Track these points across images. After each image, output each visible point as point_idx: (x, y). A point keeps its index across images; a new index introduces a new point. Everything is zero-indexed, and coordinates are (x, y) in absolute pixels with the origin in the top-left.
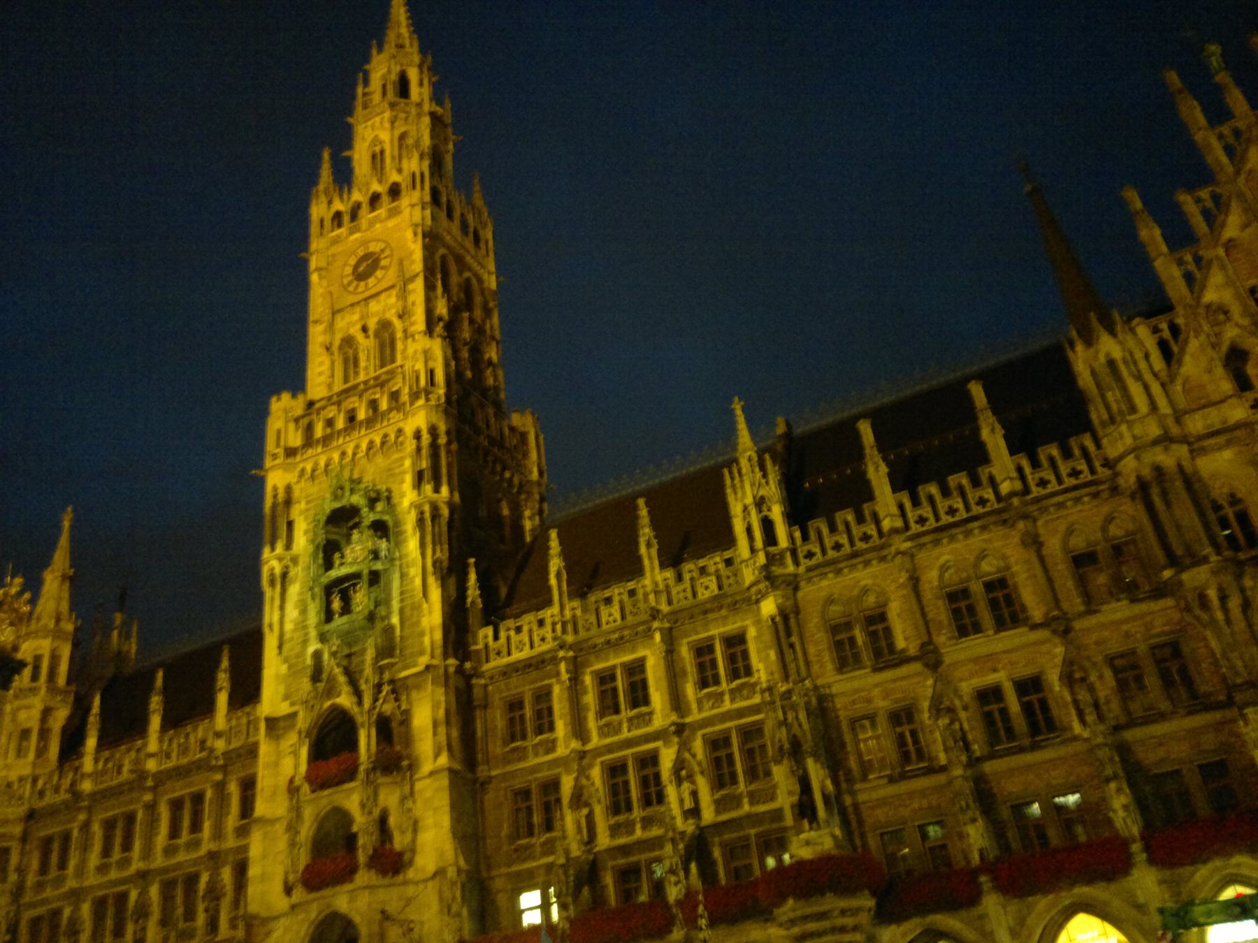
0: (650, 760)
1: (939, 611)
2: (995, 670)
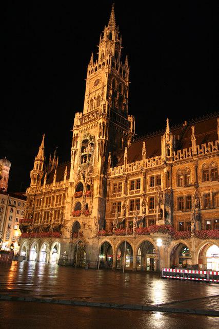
0: (139, 200)
1: (200, 175)
2: (209, 190)
